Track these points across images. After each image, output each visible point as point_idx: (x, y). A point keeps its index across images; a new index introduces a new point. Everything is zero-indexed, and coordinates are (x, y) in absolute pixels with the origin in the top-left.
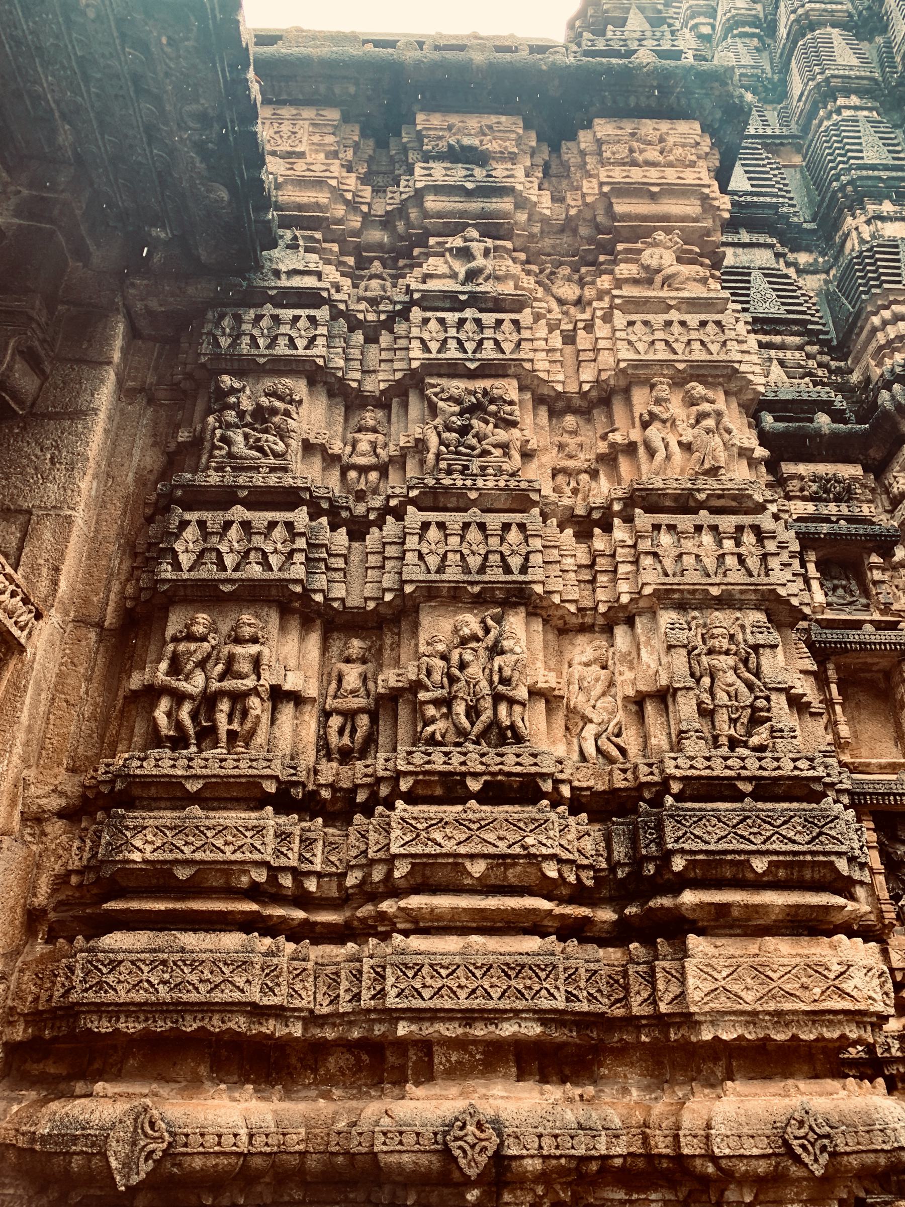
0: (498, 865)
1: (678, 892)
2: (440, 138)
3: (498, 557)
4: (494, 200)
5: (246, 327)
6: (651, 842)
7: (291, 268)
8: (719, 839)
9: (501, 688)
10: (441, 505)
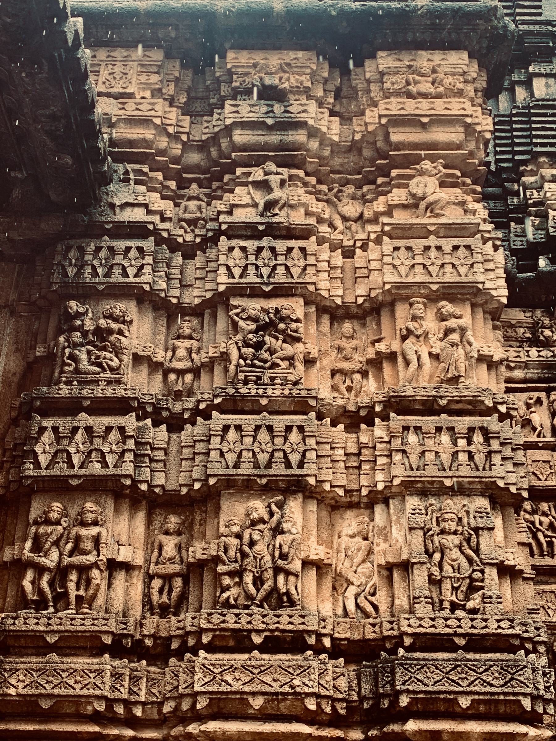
0: (273, 700)
1: (404, 721)
2: (247, 74)
3: (281, 454)
4: (290, 133)
5: (88, 257)
6: (387, 683)
7: (124, 201)
8: (435, 683)
9: (280, 562)
10: (239, 408)
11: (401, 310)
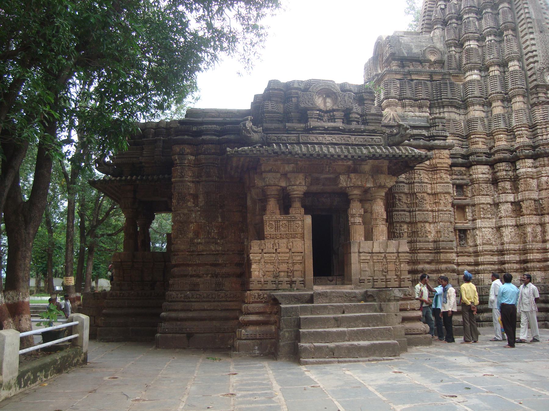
11: (439, 195)
